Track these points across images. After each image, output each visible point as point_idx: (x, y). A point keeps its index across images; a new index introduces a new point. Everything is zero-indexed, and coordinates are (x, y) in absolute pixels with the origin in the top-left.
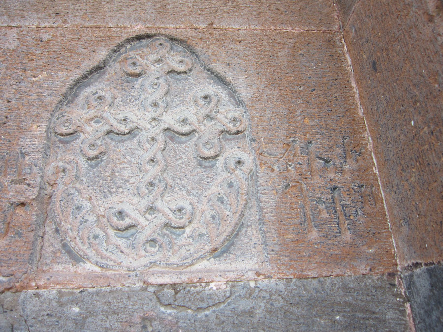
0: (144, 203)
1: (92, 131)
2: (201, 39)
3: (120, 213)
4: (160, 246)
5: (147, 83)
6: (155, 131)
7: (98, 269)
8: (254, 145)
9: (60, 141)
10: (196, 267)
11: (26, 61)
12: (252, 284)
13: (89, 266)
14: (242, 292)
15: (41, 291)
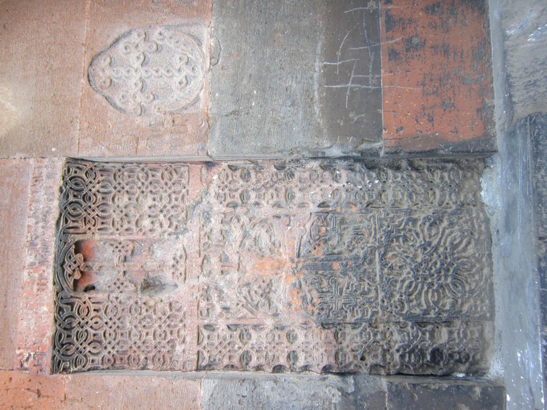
0: (176, 74)
1: (140, 98)
2: (92, 49)
3: (180, 83)
4: (195, 66)
5: (116, 76)
6: (142, 71)
7: (203, 90)
8: (153, 26)
9: (145, 112)
10: (205, 53)
11: (100, 132)
12: (213, 29)
13: (201, 94)
14: (215, 33)
15: (209, 108)
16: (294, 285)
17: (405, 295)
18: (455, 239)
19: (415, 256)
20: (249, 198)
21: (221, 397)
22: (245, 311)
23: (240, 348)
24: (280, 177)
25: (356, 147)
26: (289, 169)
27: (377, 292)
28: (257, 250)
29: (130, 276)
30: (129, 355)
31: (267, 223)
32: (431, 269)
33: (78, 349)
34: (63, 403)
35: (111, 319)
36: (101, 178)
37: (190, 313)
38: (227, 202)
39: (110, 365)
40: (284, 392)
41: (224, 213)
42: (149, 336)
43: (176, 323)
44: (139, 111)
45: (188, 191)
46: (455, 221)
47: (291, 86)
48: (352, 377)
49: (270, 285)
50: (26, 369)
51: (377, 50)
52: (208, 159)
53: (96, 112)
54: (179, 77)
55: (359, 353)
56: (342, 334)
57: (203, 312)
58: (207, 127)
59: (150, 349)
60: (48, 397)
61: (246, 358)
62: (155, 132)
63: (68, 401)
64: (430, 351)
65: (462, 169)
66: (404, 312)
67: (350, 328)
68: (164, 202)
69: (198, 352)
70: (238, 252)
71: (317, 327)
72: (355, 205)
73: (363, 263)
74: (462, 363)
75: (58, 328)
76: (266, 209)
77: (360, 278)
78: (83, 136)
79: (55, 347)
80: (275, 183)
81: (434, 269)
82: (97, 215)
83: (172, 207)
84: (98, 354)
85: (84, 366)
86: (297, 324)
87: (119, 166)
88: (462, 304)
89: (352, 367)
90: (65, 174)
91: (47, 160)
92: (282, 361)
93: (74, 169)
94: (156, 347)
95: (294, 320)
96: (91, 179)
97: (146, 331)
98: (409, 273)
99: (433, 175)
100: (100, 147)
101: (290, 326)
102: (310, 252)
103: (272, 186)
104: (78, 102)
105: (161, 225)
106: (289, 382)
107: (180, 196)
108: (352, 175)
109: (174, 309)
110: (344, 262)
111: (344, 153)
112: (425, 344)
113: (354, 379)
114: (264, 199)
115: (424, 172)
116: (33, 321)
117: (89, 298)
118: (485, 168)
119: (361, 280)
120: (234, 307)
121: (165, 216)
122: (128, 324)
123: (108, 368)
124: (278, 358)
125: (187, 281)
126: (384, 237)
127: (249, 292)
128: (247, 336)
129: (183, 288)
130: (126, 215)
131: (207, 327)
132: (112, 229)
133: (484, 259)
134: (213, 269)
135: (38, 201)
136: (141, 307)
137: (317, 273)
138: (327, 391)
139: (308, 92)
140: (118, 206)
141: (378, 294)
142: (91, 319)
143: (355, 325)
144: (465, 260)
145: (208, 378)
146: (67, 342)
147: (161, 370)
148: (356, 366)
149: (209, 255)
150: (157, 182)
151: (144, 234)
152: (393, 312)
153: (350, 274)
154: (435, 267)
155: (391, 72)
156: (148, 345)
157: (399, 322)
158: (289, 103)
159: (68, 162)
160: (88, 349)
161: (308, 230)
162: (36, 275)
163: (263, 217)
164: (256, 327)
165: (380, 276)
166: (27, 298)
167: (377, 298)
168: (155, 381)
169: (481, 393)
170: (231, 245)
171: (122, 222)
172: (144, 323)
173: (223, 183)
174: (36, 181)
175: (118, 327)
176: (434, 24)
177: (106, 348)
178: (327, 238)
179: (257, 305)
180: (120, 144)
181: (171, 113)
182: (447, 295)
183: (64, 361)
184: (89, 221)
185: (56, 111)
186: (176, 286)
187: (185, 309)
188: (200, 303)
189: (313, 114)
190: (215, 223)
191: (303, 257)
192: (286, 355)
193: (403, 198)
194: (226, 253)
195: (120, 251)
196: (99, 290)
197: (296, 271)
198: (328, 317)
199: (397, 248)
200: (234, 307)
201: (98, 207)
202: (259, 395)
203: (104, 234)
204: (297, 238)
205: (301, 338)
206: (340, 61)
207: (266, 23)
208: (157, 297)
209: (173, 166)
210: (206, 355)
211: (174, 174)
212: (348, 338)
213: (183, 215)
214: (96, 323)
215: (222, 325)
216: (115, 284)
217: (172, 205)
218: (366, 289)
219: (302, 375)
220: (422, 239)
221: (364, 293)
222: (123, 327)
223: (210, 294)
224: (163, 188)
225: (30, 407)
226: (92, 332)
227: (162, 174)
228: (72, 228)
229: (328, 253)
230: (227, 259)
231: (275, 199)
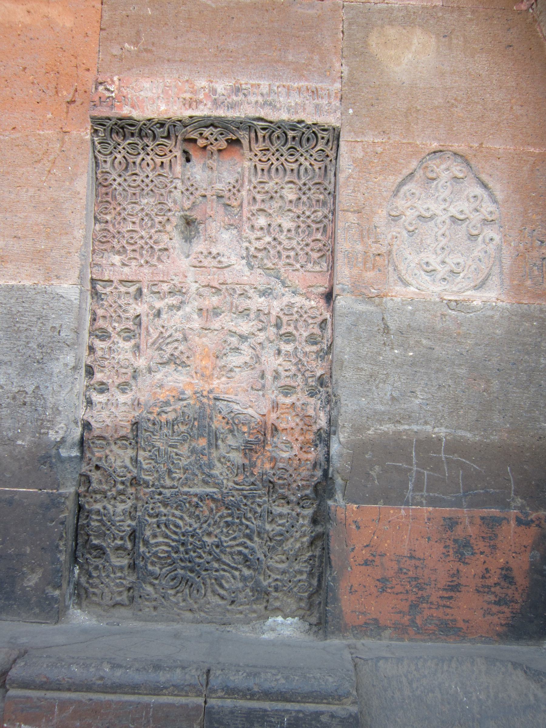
0: (439, 259)
1: (411, 214)
2: (475, 156)
3: (427, 263)
4: (448, 282)
5: (440, 185)
6: (445, 217)
7: (417, 290)
8: (501, 229)
9: (393, 220)
10: (464, 294)
11: (369, 167)
12: (494, 304)
13: (412, 289)
14: (489, 307)
15: (393, 298)
16: (183, 393)
18: (227, 582)
19: (209, 534)
20: (287, 342)
21: (59, 306)
22: (155, 336)
24: (310, 380)
26: (320, 392)
27: (171, 488)
28: (225, 350)
29: (201, 203)
31: (256, 363)
32: (194, 552)
33: (119, 145)
34: (60, 130)
35: (152, 181)
36: (316, 167)
37: (155, 272)
38: (282, 316)
39: (101, 180)
40: (62, 377)
41: (269, 313)
42: (131, 225)
43: (145, 256)
44: (394, 213)
45: (297, 270)
46: (248, 584)
47: (416, 397)
48: (78, 454)
49: (184, 364)
50: (96, 89)
51: (458, 504)
53: (395, 161)
54: (434, 262)
56: (126, 445)
57: (156, 287)
58: (370, 295)
59: (117, 226)
60: (67, 113)
61: (103, 336)
62: (366, 232)
63: (62, 134)
64: (103, 544)
65: (310, 597)
66: (147, 518)
67: (132, 455)
68: (285, 242)
69: (112, 281)
70: (223, 328)
71: (134, 417)
72: (273, 468)
73: (204, 473)
74: (88, 579)
75: (142, 123)
76: (271, 362)
77: (187, 469)
78: (366, 146)
80: (303, 375)
81: (194, 555)
82: (272, 164)
83: (279, 252)
84: (114, 167)
86: (138, 395)
87: (331, 188)
88: (153, 585)
89: (88, 455)
90: (320, 126)
91: (337, 104)
92: (99, 376)
94: (119, 232)
95: (143, 390)
96: (315, 156)
97: (137, 222)
99: (305, 561)
100: (352, 167)
101: (137, 386)
102: (220, 412)
103: (299, 370)
105: (258, 239)
106: (72, 383)
107: (291, 261)
108: (309, 466)
109: (160, 253)
110: (206, 452)
112: (110, 539)
113: (76, 457)
115: (308, 552)
116: (150, 94)
117: (176, 157)
118: (310, 624)
119: (185, 470)
120: (161, 322)
121: (269, 243)
122: (146, 201)
123: (97, 179)
124: (102, 371)
125: (193, 269)
126: (232, 499)
127: (177, 340)
128: (127, 336)
129: (184, 263)
130: (272, 198)
131: (140, 292)
132: (254, 181)
133: (203, 614)
134: (204, 299)
135: (288, 95)
136: (164, 215)
137: (195, 419)
138: (62, 425)
139: (409, 417)
140: (282, 188)
141: (168, 488)
142: (152, 159)
143: (135, 461)
144: (203, 592)
145: (81, 292)
146: (126, 133)
147: (93, 239)
148: (90, 459)
149: (221, 295)
151: (249, 219)
153: (193, 458)
155: (429, 519)
156: (122, 224)
157: (136, 511)
158: (396, 394)
159: (334, 129)
160: (119, 156)
161: (245, 411)
162: (201, 97)
164: (137, 347)
166: (176, 86)
167: (163, 487)
168: (79, 233)
169: (52, 596)
170: (232, 321)
171: (264, 193)
172: (146, 219)
173: (306, 312)
174: (313, 92)
176: (487, 575)
177: (120, 176)
178: (236, 433)
179: (162, 349)
180: (354, 191)
181: (390, 252)
182: (164, 567)
183: (105, 130)
184: (265, 155)
185: (398, 113)
186: (188, 256)
187: (160, 266)
188: (166, 284)
189: (381, 422)
190: (260, 302)
191: (215, 404)
192: (105, 381)
193: (279, 525)
194: (223, 315)
195: (230, 190)
196: (185, 166)
197: (198, 395)
201: (282, 164)
202: (60, 349)
203: (249, 172)
205: (122, 398)
206: (446, 458)
207: (498, 370)
208: (175, 234)
210: (108, 290)
212: (121, 452)
213: (270, 265)
214: (148, 165)
215: (140, 308)
218: (174, 475)
219: (82, 398)
220: (230, 543)
221: (170, 472)
222: (143, 195)
225: (57, 92)
226: (138, 160)
227: (319, 240)
230: (217, 315)
231: (284, 374)
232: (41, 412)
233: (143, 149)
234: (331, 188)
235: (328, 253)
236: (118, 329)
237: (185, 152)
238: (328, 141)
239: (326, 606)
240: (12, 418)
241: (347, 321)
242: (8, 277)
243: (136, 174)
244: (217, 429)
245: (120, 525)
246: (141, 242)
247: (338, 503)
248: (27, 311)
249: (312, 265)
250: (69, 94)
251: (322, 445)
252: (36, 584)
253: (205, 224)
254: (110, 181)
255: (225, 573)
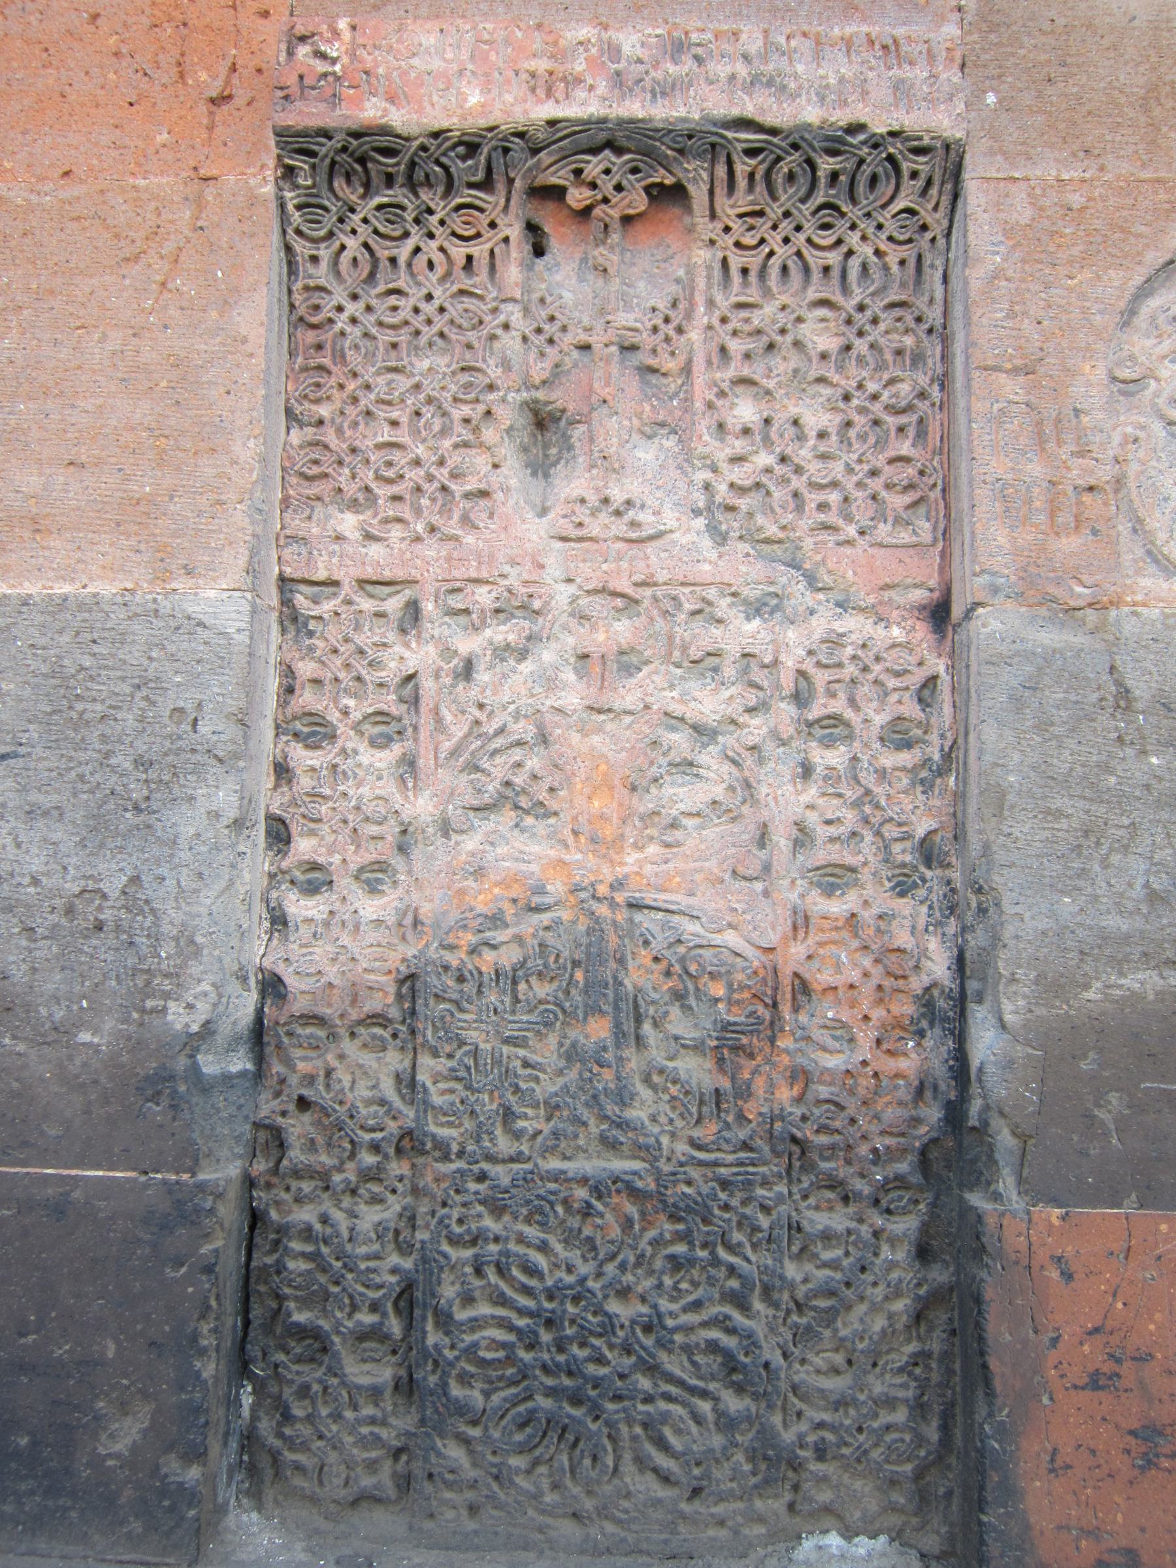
16: (540, 890)
17: (500, 1253)
18: (678, 1432)
19: (624, 1293)
20: (828, 743)
21: (194, 652)
22: (459, 731)
23: (346, 713)
24: (897, 848)
25: (1002, 1113)
26: (924, 880)
27: (512, 1160)
28: (654, 769)
29: (575, 365)
30: (334, 369)
31: (744, 802)
32: (583, 1345)
33: (353, 211)
34: (192, 174)
35: (442, 310)
36: (892, 260)
39: (302, 311)
40: (204, 849)
41: (776, 662)
42: (387, 429)
43: (426, 513)
44: (1125, 374)
45: (849, 542)
46: (739, 1438)
48: (249, 1066)
49: (541, 810)
50: (290, 53)
52: (957, 611)
53: (1123, 230)
55: (318, 1093)
56: (382, 1039)
57: (460, 596)
58: (1072, 603)
59: (348, 433)
60: (211, 128)
61: (314, 734)
62: (1053, 427)
63: (196, 185)
64: (321, 1322)
65: (919, 1475)
66: (446, 1248)
67: (400, 1068)
68: (813, 468)
69: (336, 584)
70: (647, 707)
71: (404, 960)
72: (799, 1100)
73: (607, 1117)
74: (280, 1425)
75: (416, 144)
76: (786, 799)
77: (557, 1107)
78: (1038, 191)
79: (357, 135)
80: (878, 834)
82: (771, 254)
83: (796, 495)
84: (338, 274)
85: (299, 232)
86: (415, 896)
87: (934, 315)
88: (465, 1441)
89: (277, 1068)
90: (908, 139)
91: (955, 80)
92: (303, 846)
93: (926, 168)
94: (354, 450)
95: (430, 886)
96: (891, 227)
97: (404, 420)
98: (570, 1269)
99: (901, 1370)
100: (1002, 249)
102: (646, 943)
103: (866, 821)
104: (1156, 170)
105: (738, 459)
106: (233, 866)
107: (832, 518)
108: (904, 1094)
109: (468, 505)
110: (609, 1056)
111: (980, 1070)
112: (341, 1309)
113: (243, 1074)
114: (824, 794)
115: (909, 1341)
116: (436, 64)
117: (506, 240)
118: (923, 1556)
119: (552, 1109)
120: (474, 693)
121: (768, 470)
122: (426, 364)
123: (292, 306)
124: (312, 833)
125: (559, 545)
126: (688, 1190)
127: (519, 743)
128: (381, 735)
129: (536, 531)
130: (771, 346)
131: (413, 610)
132: (724, 302)
133: (610, 1527)
134: (594, 628)
135: (818, 57)
136: (477, 401)
137: (576, 964)
138: (205, 986)
140: (799, 320)
141: (504, 1161)
142: (442, 249)
143: (408, 1083)
145: (254, 612)
146: (373, 174)
147: (283, 469)
148: (283, 1081)
149: (639, 615)
150: (881, 444)
151: (710, 406)
152: (446, 1210)
153: (572, 1075)
154: (589, 1359)
157: (414, 1227)
158: (1160, 883)
159: (947, 147)
160: (352, 243)
161: (717, 939)
162: (579, 66)
163: (764, 790)
164: (409, 763)
165: (564, 1172)
166: (507, 42)
167: (490, 1158)
168: (247, 449)
169: (181, 1484)
170: (672, 687)
172: (428, 412)
173: (878, 659)
174: (885, 47)
175: (418, 333)
177: (355, 297)
178: (692, 1001)
179: (477, 769)
180: (1011, 315)
181: (1119, 482)
185: (1123, 100)
186: (543, 512)
187: (469, 539)
188: (486, 588)
189: (1120, 964)
190: (744, 632)
191: (631, 920)
192: (320, 860)
193: (825, 1265)
194: (646, 670)
195: (655, 330)
196: (530, 268)
197: (583, 895)
198: (436, 996)
199: (652, 1233)
200: (474, 693)
201: (799, 254)
202: (198, 770)
204: (692, 901)
205: (370, 908)
208: (508, 452)
209: (936, 494)
210: (327, 607)
211: (908, 499)
212: (368, 1059)
213: (772, 530)
215: (417, 656)
216: (552, 319)
217: (804, 491)
218: (521, 1124)
219: (259, 908)
220: (685, 1318)
221: (508, 1115)
222: (417, 348)
223: (513, 616)
224: (860, 461)
225: (182, 75)
226: (404, 252)
227: (906, 460)
228: (731, 173)
229: (641, 1002)
230: (629, 670)
231: (823, 832)
232: (144, 950)
233: (417, 221)
234: (934, 315)
235: (932, 495)
236: (356, 716)
237: (532, 228)
238: (929, 183)
239: (981, 1510)
240: (63, 969)
241: (1010, 678)
242: (51, 574)
243: (397, 292)
244: (639, 990)
245: (368, 1270)
246: (415, 475)
247: (1006, 1205)
248: (106, 667)
249: (889, 527)
250: (215, 77)
251: (938, 1031)
252: (134, 1448)
253: (588, 422)
254: (327, 312)
255: (672, 1407)
